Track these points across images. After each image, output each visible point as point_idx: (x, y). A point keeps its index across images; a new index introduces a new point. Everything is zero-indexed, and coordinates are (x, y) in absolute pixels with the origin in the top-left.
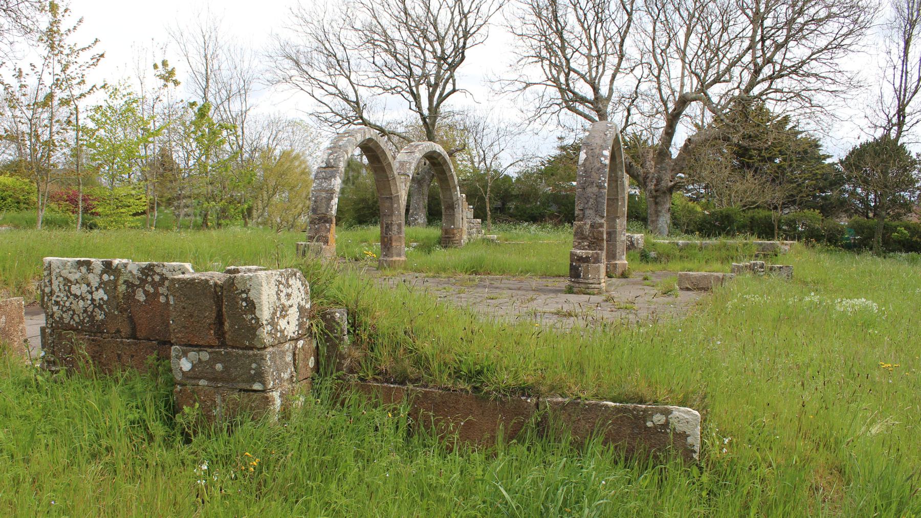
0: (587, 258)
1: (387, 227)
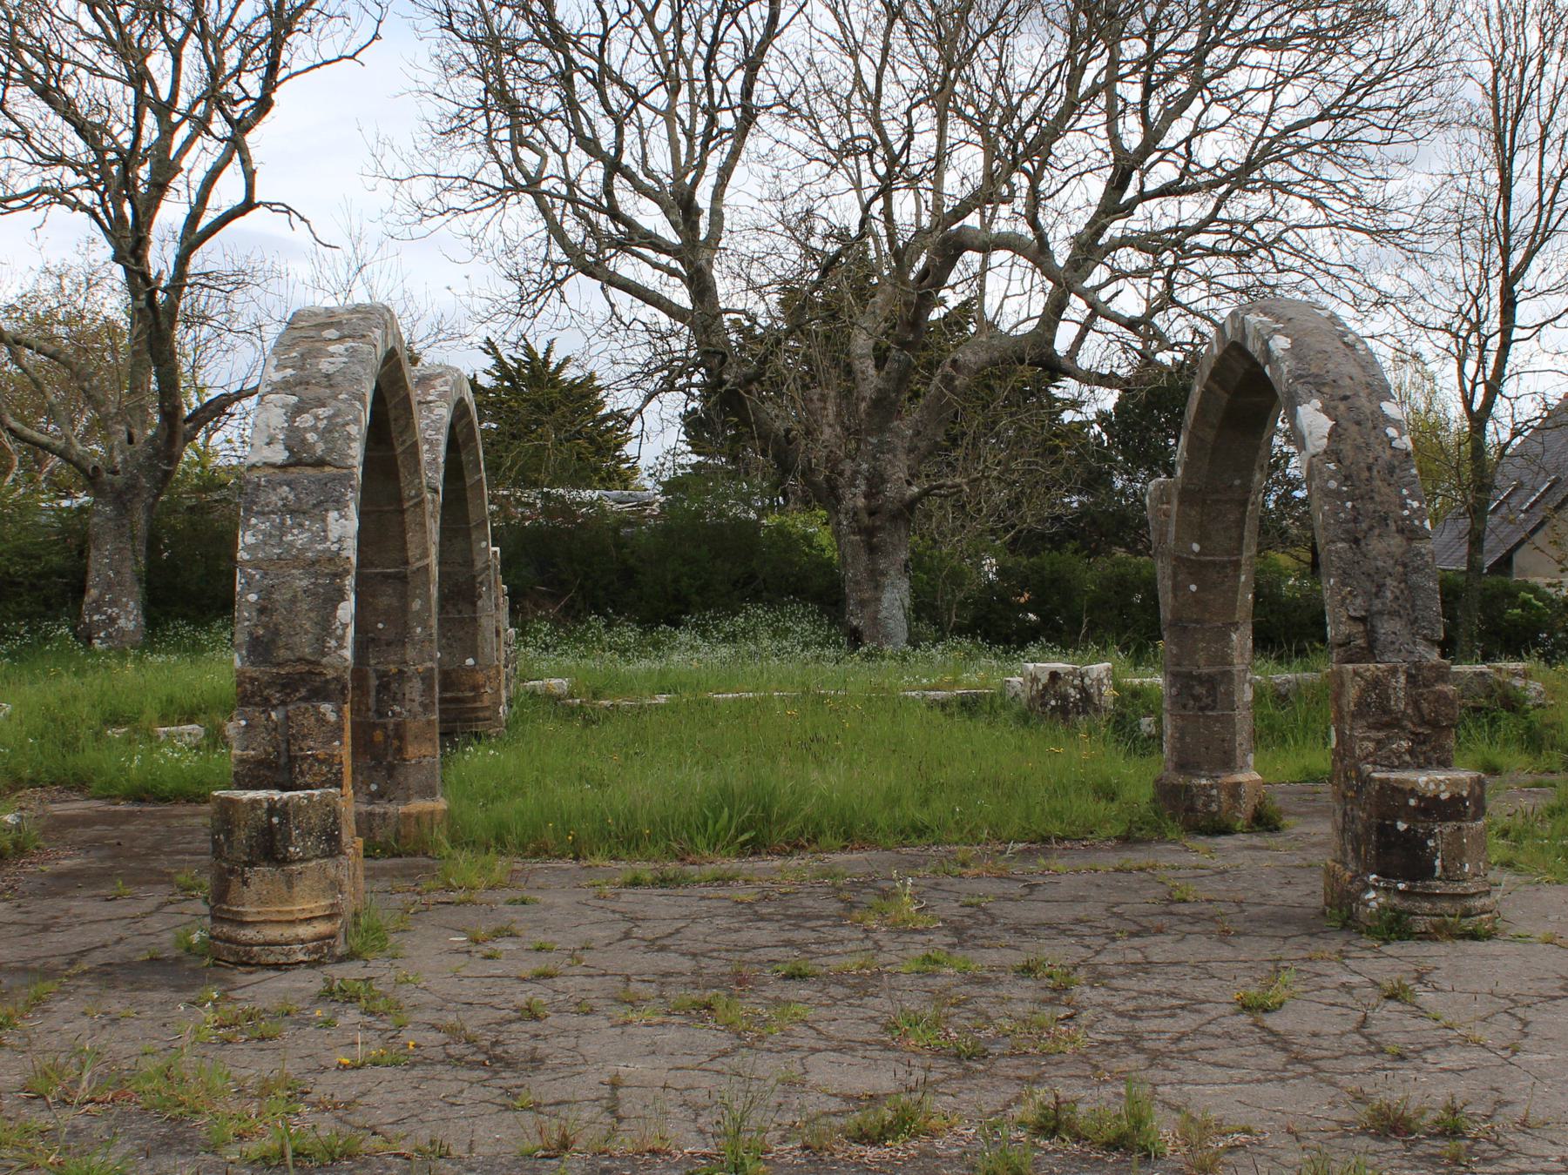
0: (1456, 800)
1: (384, 687)
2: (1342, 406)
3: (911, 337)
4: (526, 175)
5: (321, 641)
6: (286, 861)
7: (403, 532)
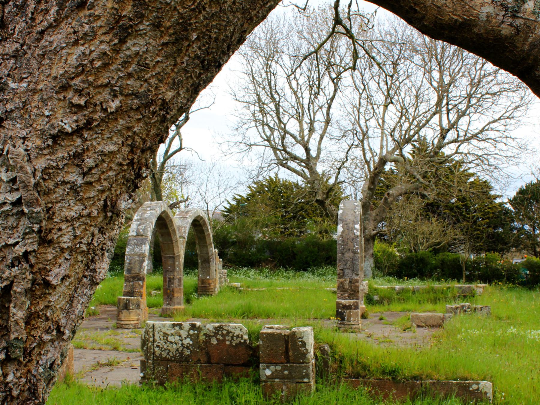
0: (350, 306)
1: (170, 281)
2: (346, 226)
3: (372, 187)
4: (267, 136)
5: (140, 270)
6: (129, 309)
7: (173, 248)
